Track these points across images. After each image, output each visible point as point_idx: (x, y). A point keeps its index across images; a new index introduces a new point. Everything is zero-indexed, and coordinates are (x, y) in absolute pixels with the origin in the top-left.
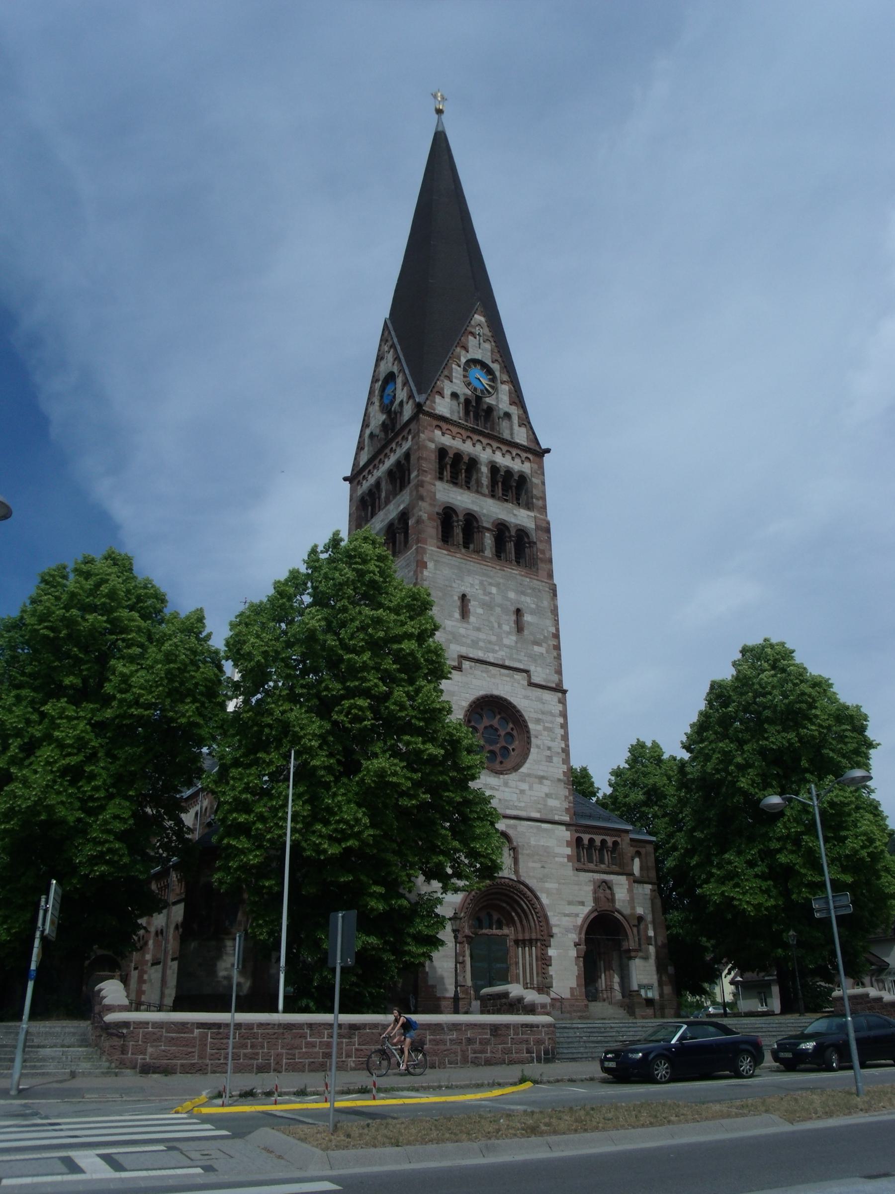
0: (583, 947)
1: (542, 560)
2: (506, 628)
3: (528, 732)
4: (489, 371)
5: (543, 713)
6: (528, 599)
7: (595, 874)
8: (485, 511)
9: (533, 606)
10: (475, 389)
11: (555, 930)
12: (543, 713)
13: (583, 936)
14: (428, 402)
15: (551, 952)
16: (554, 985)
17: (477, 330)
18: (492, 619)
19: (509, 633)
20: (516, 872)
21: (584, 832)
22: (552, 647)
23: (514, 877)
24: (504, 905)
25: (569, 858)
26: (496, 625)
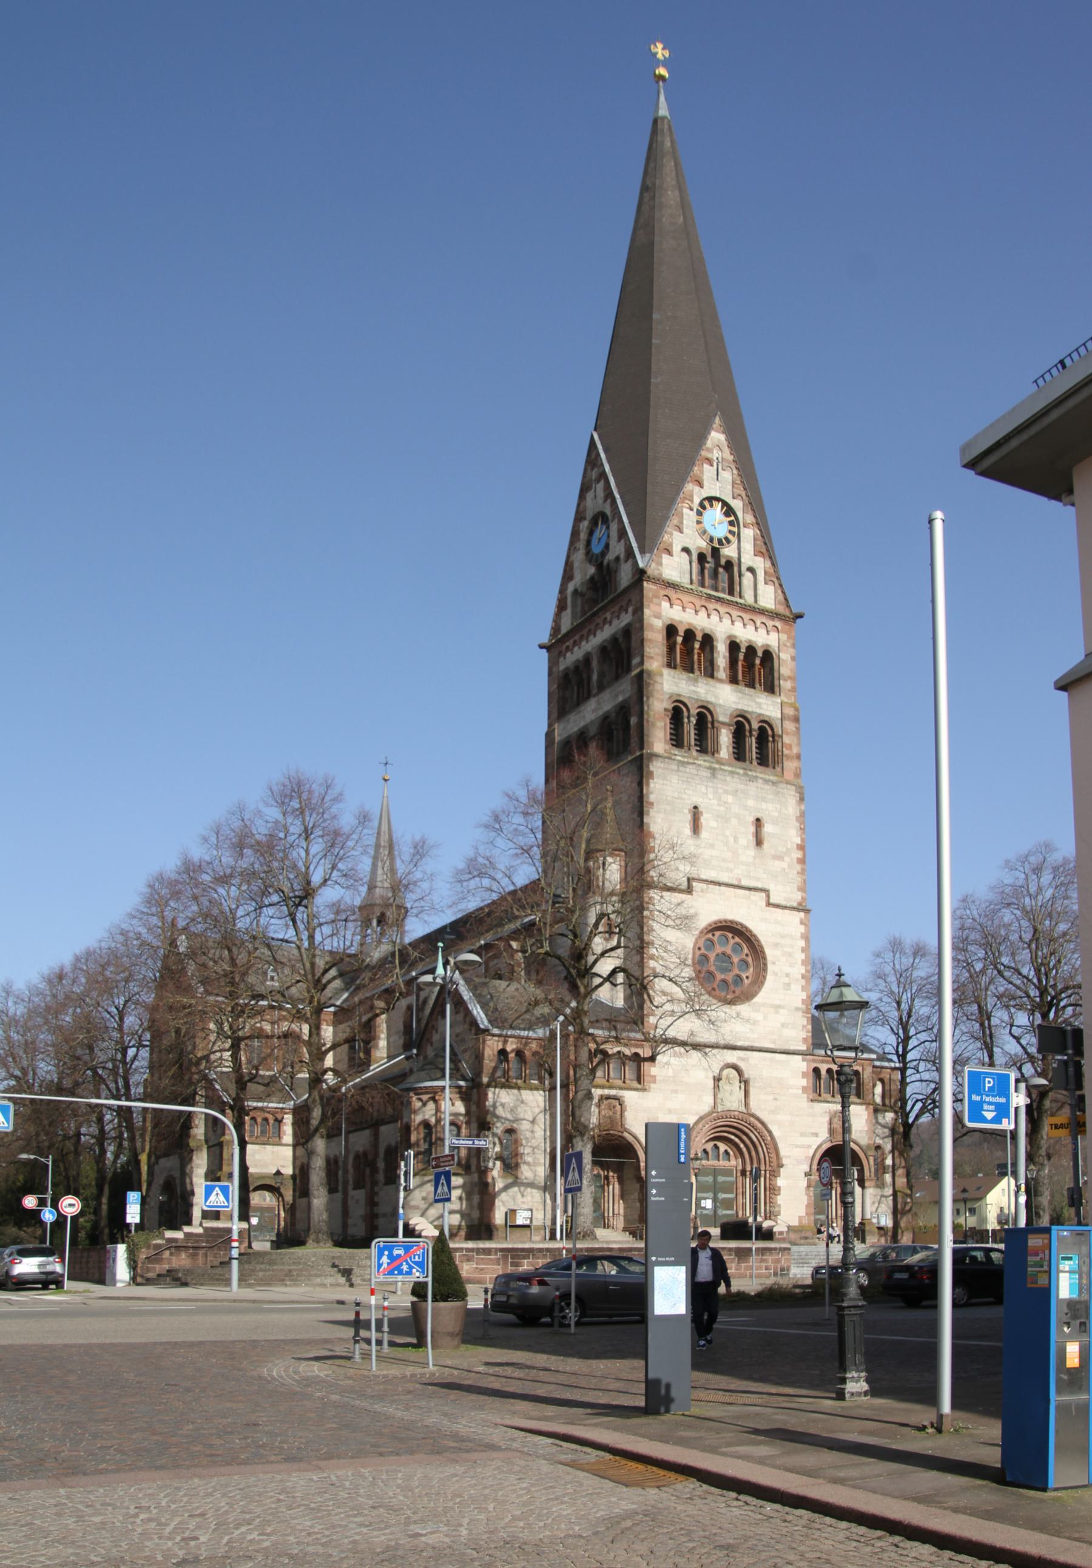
0: (815, 1177)
1: (788, 757)
2: (743, 841)
3: (765, 958)
4: (729, 511)
5: (782, 937)
6: (770, 806)
7: (830, 1105)
8: (721, 702)
9: (776, 814)
10: (711, 540)
11: (784, 1161)
12: (782, 937)
13: (815, 1167)
14: (653, 565)
16: (782, 1213)
17: (715, 454)
18: (728, 833)
20: (746, 1105)
21: (823, 1062)
22: (795, 861)
23: (743, 1109)
24: (733, 1137)
25: (804, 1089)
26: (731, 840)
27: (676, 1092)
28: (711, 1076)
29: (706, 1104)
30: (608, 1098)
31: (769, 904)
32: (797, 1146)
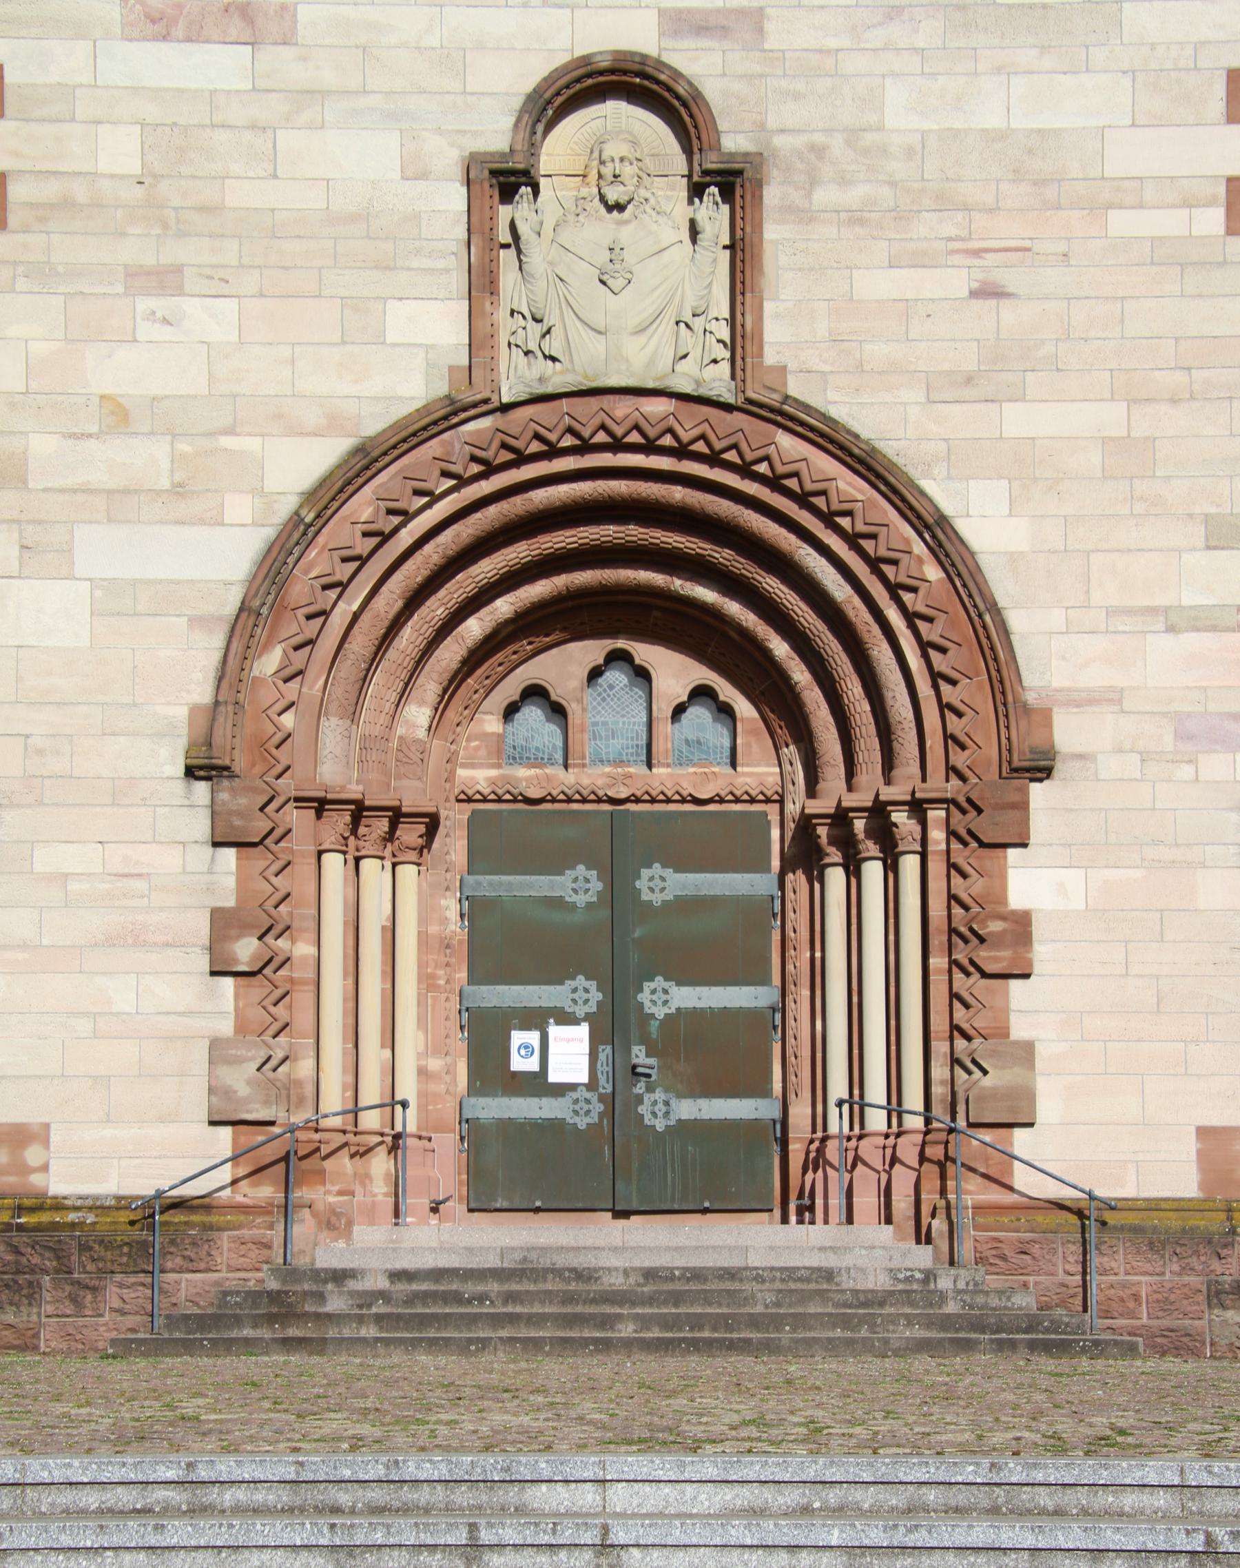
11: (1067, 733)
15: (1027, 882)
16: (1047, 1108)
23: (717, 380)
27: (166, 280)
28: (447, 158)
29: (409, 351)
32: (1175, 621)
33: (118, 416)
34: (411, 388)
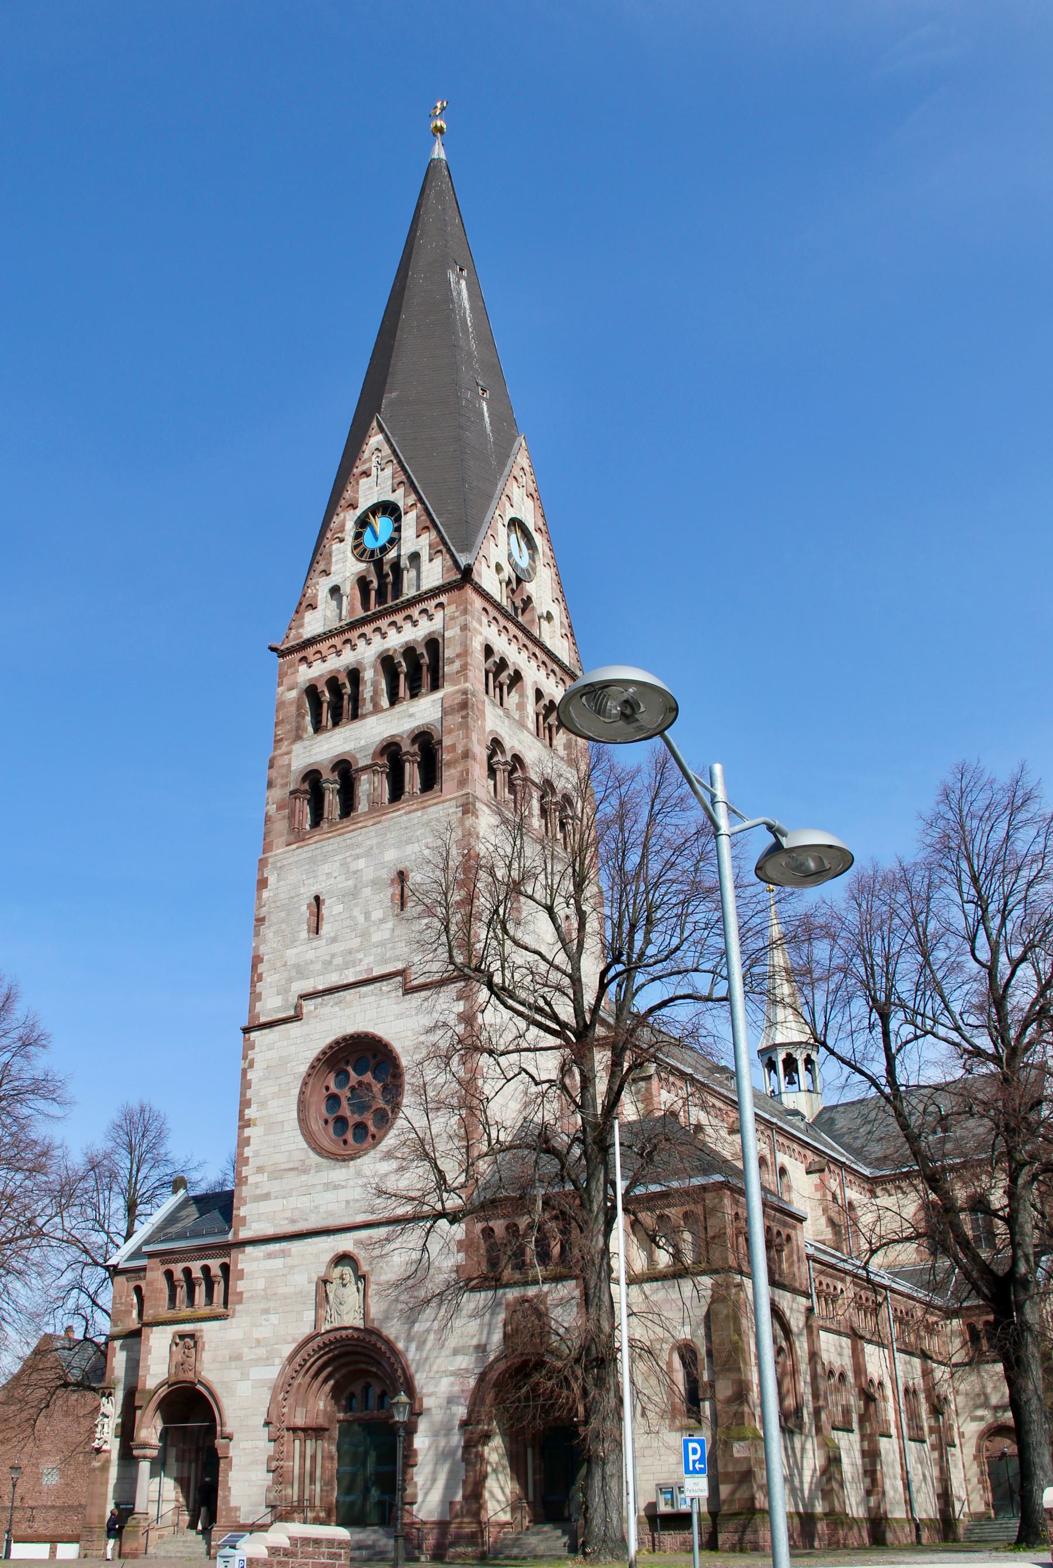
2: (377, 914)
19: (382, 921)
26: (361, 919)
27: (266, 1311)
28: (315, 1279)
30: (182, 1337)
31: (409, 991)
33: (258, 1342)
34: (307, 1330)
